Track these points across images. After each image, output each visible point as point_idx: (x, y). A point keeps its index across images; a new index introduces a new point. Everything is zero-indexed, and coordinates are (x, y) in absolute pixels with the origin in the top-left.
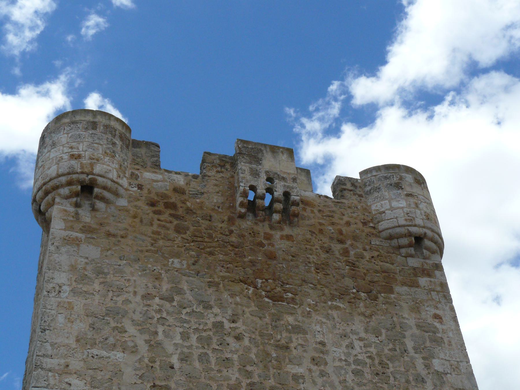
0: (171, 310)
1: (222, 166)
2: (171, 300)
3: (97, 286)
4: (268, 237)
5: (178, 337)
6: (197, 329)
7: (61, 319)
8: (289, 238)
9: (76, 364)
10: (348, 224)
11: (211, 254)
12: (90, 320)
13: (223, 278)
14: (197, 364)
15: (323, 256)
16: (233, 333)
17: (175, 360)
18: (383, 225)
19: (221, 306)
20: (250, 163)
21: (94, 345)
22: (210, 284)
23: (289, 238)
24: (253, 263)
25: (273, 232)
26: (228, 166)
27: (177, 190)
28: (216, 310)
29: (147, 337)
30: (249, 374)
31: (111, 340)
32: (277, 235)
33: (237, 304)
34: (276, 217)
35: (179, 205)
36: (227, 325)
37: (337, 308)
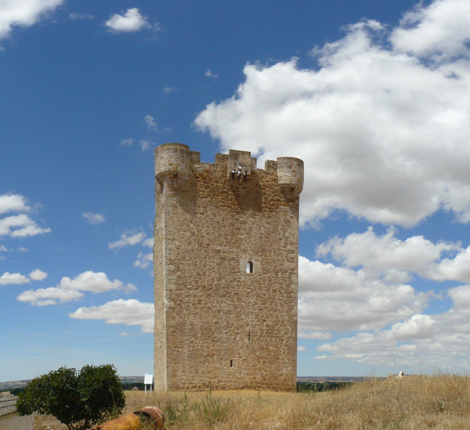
0: (203, 217)
1: (223, 159)
2: (203, 214)
3: (180, 210)
4: (237, 188)
5: (206, 226)
6: (211, 224)
7: (170, 223)
8: (245, 188)
9: (176, 236)
10: (267, 181)
11: (217, 196)
12: (180, 222)
13: (221, 206)
14: (211, 236)
15: (256, 194)
16: (223, 225)
17: (205, 235)
18: (280, 182)
19: (219, 215)
20: (234, 160)
21: (180, 230)
22: (217, 207)
23: (245, 188)
24: (231, 199)
25: (239, 186)
26: (225, 159)
27: (207, 171)
28: (218, 217)
29: (196, 227)
30: (226, 238)
31: (186, 229)
32: (240, 187)
33: (225, 215)
34: (241, 181)
35: (207, 178)
36: (221, 222)
37: (258, 215)
